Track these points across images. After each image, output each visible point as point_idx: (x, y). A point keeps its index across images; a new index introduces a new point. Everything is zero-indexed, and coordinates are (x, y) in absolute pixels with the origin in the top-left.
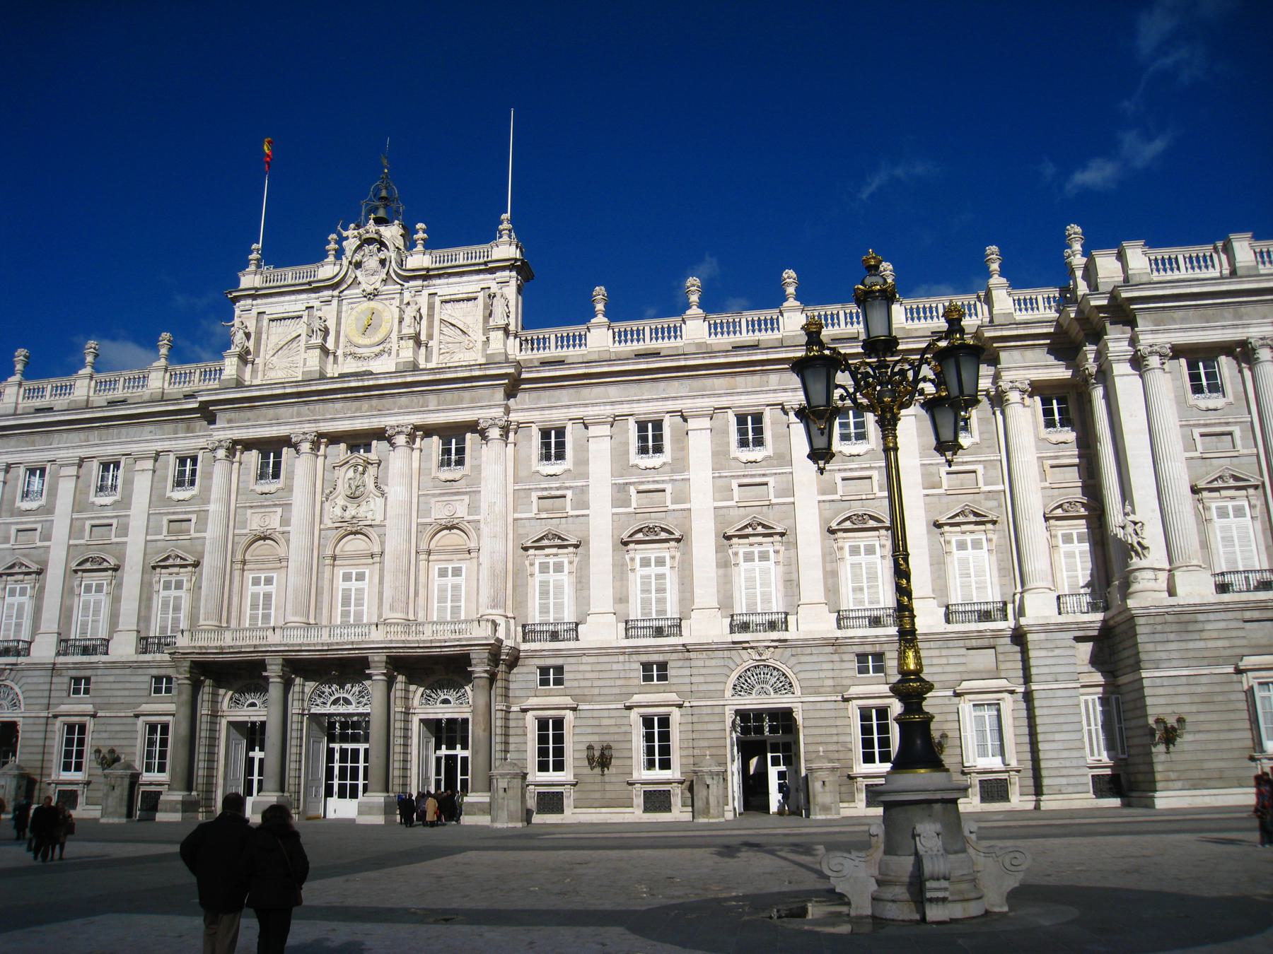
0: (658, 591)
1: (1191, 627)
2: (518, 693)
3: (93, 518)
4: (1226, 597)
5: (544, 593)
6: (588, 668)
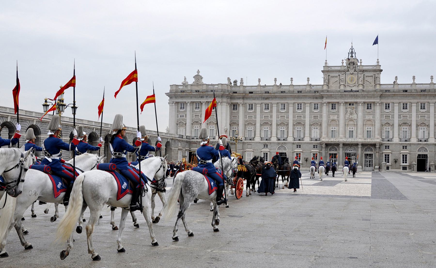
2: (381, 150)
6: (394, 146)
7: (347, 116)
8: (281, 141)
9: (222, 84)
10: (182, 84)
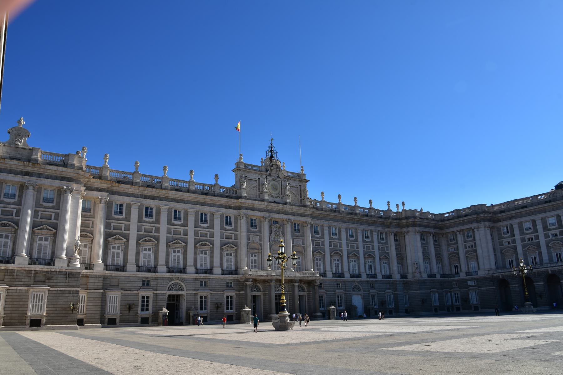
4: (429, 278)
5: (317, 266)
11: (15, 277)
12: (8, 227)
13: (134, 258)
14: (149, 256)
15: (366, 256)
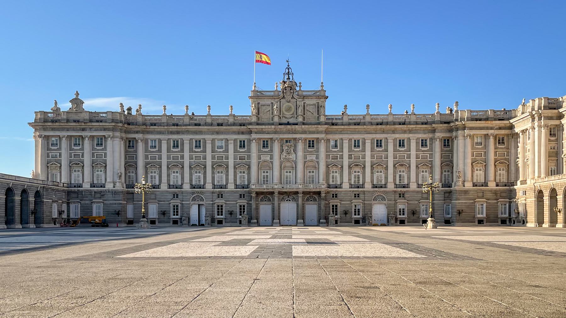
0: (358, 178)
1: (467, 193)
3: (217, 155)
4: (474, 187)
5: (333, 178)
7: (283, 156)
8: (196, 190)
9: (112, 112)
10: (52, 111)
11: (84, 195)
12: (78, 165)
13: (166, 178)
14: (177, 177)
15: (396, 166)
